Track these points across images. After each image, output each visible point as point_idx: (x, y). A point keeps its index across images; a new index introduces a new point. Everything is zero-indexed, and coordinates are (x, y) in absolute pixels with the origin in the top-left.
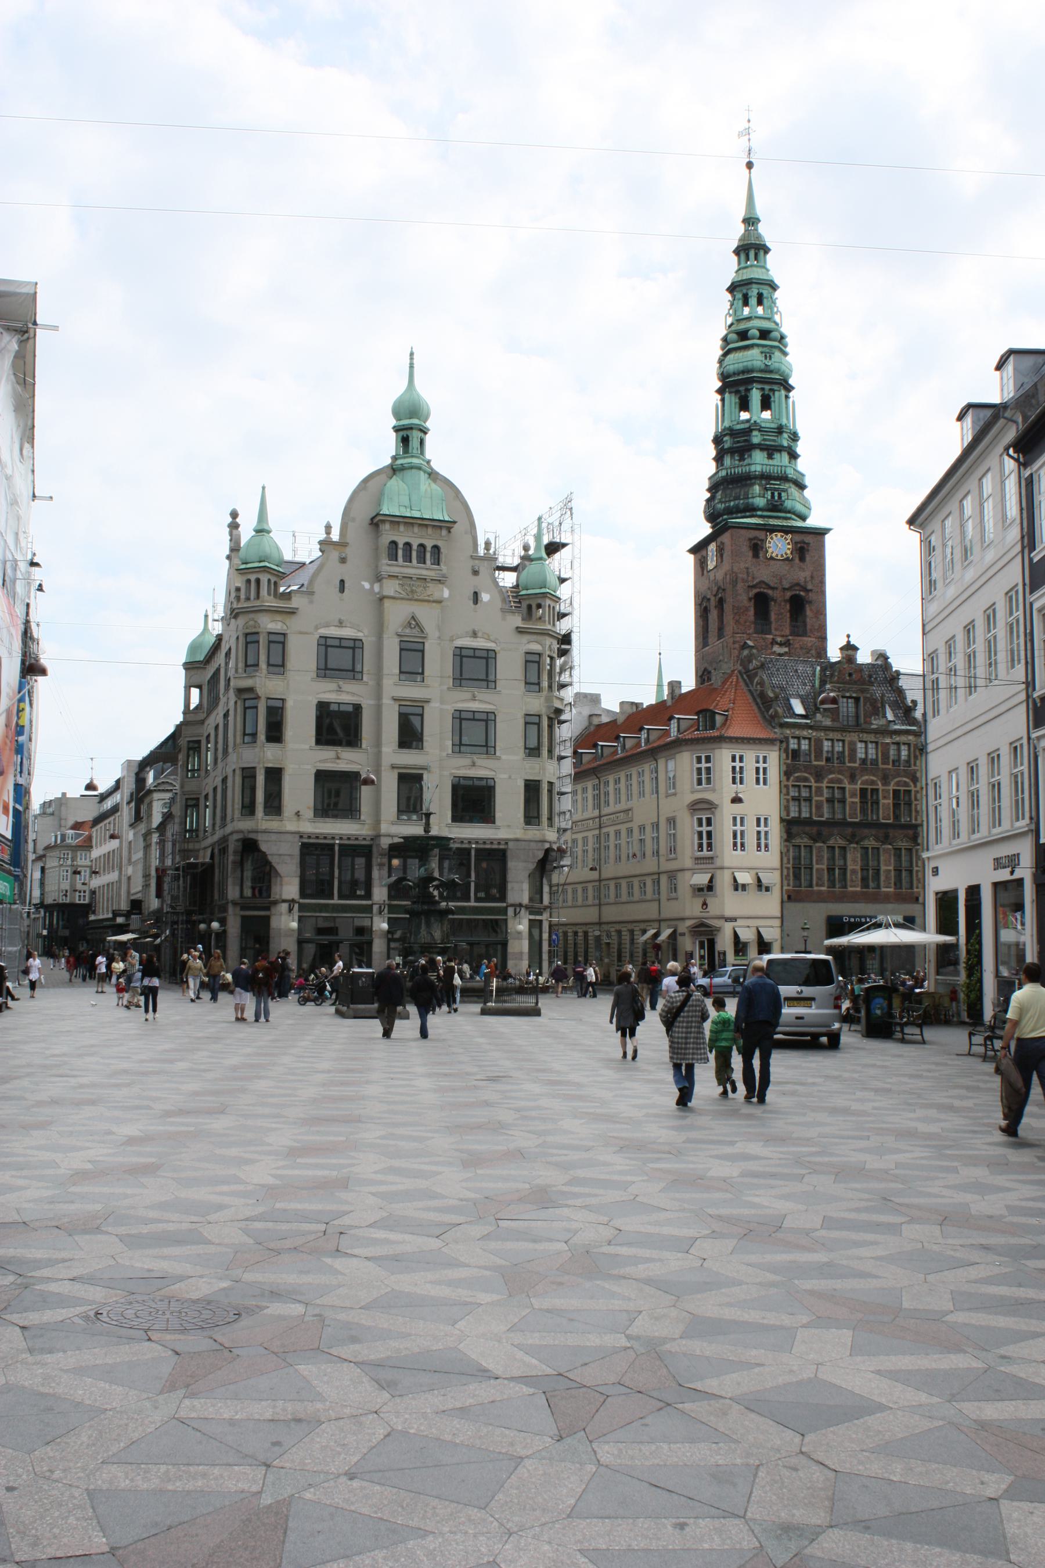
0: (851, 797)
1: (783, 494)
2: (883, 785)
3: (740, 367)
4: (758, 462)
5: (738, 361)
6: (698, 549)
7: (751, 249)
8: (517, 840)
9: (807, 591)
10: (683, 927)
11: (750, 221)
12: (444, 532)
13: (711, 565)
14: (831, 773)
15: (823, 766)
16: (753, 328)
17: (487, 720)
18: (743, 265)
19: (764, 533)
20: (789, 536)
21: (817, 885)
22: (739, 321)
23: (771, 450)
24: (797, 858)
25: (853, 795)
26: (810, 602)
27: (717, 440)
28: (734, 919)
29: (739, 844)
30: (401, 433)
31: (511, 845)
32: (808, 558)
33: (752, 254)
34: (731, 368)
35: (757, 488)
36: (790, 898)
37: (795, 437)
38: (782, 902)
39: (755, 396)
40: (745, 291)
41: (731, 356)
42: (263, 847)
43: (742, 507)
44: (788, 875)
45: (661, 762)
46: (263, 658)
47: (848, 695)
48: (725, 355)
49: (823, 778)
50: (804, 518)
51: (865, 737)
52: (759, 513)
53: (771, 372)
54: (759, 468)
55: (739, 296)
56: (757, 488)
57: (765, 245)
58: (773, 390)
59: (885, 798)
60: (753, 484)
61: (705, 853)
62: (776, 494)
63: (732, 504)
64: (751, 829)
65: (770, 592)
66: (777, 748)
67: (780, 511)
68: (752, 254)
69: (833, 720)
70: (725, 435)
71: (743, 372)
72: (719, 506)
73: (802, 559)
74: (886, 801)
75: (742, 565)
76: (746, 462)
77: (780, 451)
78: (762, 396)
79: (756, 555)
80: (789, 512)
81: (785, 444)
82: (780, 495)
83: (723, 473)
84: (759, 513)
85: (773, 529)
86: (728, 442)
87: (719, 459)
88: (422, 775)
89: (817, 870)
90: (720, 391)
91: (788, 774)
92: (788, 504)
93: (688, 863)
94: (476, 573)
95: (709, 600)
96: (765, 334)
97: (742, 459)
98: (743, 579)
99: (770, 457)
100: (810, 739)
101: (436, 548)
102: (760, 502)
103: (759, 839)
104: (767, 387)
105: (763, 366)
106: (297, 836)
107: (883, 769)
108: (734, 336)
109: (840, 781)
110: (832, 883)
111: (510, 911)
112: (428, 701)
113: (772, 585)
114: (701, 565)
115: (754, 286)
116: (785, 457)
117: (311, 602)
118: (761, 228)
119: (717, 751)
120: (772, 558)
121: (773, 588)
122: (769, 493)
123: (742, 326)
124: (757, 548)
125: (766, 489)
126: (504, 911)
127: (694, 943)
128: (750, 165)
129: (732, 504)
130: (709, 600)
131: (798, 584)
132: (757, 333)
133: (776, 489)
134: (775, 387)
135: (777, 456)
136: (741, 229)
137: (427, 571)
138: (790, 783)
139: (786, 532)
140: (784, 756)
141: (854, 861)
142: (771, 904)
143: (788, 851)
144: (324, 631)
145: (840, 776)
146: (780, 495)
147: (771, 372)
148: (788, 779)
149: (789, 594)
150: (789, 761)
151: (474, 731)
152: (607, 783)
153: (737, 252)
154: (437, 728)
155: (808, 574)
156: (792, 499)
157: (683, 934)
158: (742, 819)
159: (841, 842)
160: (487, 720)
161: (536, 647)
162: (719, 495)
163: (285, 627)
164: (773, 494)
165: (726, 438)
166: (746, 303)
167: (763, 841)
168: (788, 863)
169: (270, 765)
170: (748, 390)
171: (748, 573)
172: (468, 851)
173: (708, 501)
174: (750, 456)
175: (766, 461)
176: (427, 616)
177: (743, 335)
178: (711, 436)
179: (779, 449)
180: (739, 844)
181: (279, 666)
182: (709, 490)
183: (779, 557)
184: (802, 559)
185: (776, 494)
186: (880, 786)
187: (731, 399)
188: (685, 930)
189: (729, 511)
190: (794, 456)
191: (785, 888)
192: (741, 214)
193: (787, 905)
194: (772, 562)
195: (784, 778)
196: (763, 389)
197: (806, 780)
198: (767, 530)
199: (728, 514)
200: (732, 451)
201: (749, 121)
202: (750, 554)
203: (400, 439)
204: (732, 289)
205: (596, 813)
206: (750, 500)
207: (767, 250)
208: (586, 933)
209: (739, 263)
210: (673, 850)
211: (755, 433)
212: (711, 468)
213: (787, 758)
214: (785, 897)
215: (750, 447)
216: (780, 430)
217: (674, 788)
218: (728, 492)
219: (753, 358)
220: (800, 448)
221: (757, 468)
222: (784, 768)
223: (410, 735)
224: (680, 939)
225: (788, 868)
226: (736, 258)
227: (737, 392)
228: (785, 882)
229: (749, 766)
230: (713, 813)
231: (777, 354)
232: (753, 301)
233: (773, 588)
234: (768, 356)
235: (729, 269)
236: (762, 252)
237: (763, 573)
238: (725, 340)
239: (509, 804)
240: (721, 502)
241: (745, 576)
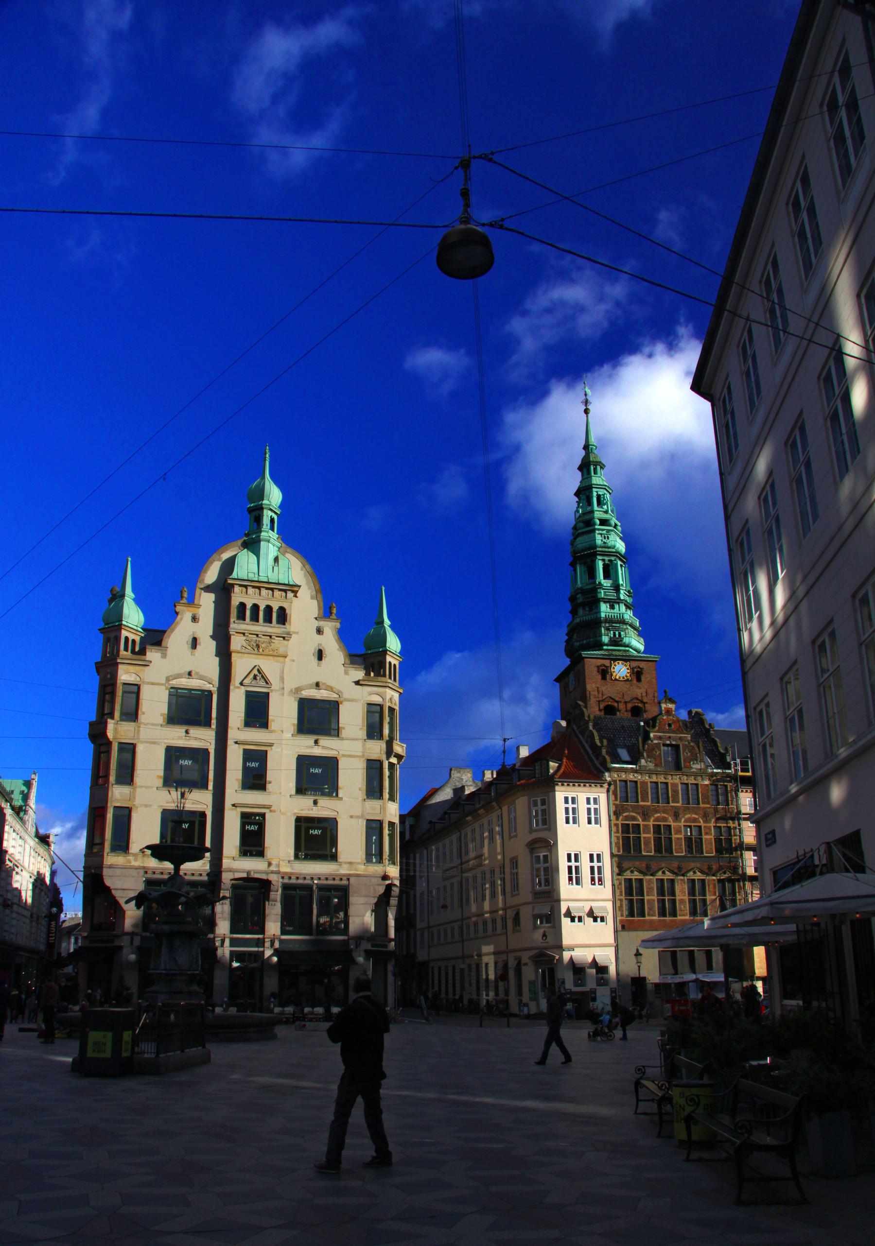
0: (676, 834)
2: (704, 822)
3: (586, 545)
8: (358, 876)
9: (644, 703)
10: (525, 957)
12: (290, 595)
13: (571, 688)
14: (657, 812)
15: (649, 806)
17: (330, 765)
21: (649, 915)
23: (612, 603)
24: (629, 891)
25: (678, 831)
26: (645, 711)
27: (572, 599)
28: (571, 949)
29: (575, 877)
30: (254, 514)
31: (352, 880)
32: (643, 678)
34: (580, 546)
36: (623, 927)
38: (616, 931)
39: (600, 565)
41: (580, 540)
42: (108, 882)
44: (621, 906)
45: (505, 809)
46: (118, 707)
47: (668, 742)
49: (650, 817)
51: (685, 779)
53: (609, 548)
55: (583, 497)
57: (600, 462)
59: (706, 834)
61: (543, 888)
64: (585, 865)
65: (616, 705)
66: (605, 790)
69: (656, 765)
70: (577, 594)
74: (708, 837)
79: (604, 678)
80: (627, 646)
82: (620, 634)
83: (578, 620)
87: (574, 612)
88: (263, 815)
89: (648, 901)
90: (573, 565)
91: (617, 814)
92: (626, 640)
93: (529, 897)
94: (319, 631)
96: (604, 522)
97: (591, 610)
99: (612, 607)
100: (636, 782)
101: (282, 611)
103: (592, 872)
104: (606, 558)
106: (142, 871)
107: (704, 808)
108: (581, 525)
109: (665, 819)
110: (662, 913)
112: (271, 745)
113: (617, 699)
114: (565, 692)
117: (164, 656)
120: (616, 680)
121: (617, 702)
123: (587, 517)
124: (605, 673)
127: (537, 972)
128: (586, 411)
132: (598, 522)
137: (274, 629)
138: (620, 822)
139: (626, 661)
140: (612, 797)
141: (682, 891)
142: (605, 932)
143: (620, 884)
144: (175, 683)
145: (666, 816)
146: (620, 634)
147: (609, 548)
148: (617, 819)
149: (629, 706)
150: (618, 802)
151: (317, 776)
152: (466, 835)
154: (282, 773)
155: (643, 691)
157: (526, 964)
158: (576, 856)
159: (669, 875)
160: (330, 765)
161: (377, 699)
162: (575, 637)
163: (138, 679)
164: (614, 634)
165: (579, 596)
166: (589, 502)
167: (596, 876)
168: (621, 895)
169: (118, 805)
172: (309, 888)
173: (567, 641)
176: (269, 667)
179: (618, 601)
180: (575, 877)
181: (132, 715)
184: (639, 680)
186: (702, 824)
188: (527, 961)
191: (618, 918)
192: (583, 443)
193: (624, 934)
195: (613, 817)
196: (603, 560)
197: (634, 819)
198: (611, 659)
200: (583, 605)
202: (600, 677)
203: (253, 518)
204: (577, 494)
205: (459, 862)
208: (454, 968)
209: (582, 476)
210: (516, 886)
213: (616, 799)
214: (619, 928)
216: (617, 588)
217: (516, 831)
222: (613, 808)
223: (256, 777)
224: (524, 968)
225: (621, 900)
226: (580, 473)
227: (585, 563)
228: (619, 913)
229: (582, 807)
230: (550, 851)
235: (575, 481)
237: (609, 690)
239: (351, 843)
240: (577, 641)
241: (596, 693)
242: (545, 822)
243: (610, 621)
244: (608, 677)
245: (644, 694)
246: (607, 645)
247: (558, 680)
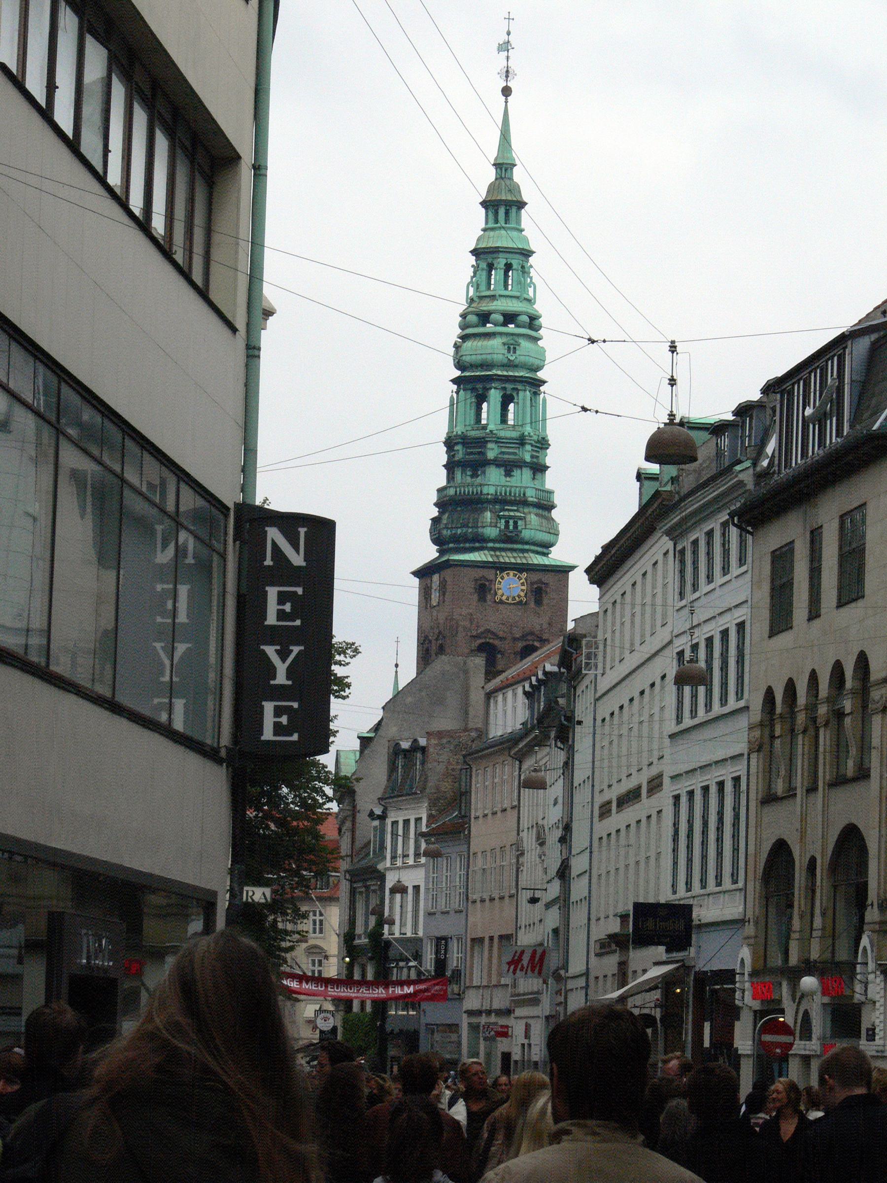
1: (520, 523)
4: (493, 481)
5: (476, 349)
6: (423, 573)
7: (503, 204)
11: (504, 168)
16: (495, 312)
18: (491, 225)
19: (493, 571)
20: (524, 575)
22: (481, 298)
23: (509, 467)
27: (450, 443)
32: (545, 601)
33: (502, 211)
35: (488, 515)
37: (543, 444)
40: (490, 261)
41: (469, 344)
48: (464, 338)
50: (545, 547)
52: (490, 545)
54: (492, 490)
55: (484, 265)
56: (488, 515)
58: (517, 390)
60: (485, 509)
62: (511, 522)
63: (459, 531)
65: (497, 642)
67: (516, 542)
68: (502, 211)
72: (445, 532)
73: (539, 602)
75: (465, 611)
76: (479, 480)
77: (521, 467)
78: (503, 397)
79: (482, 598)
81: (528, 458)
82: (515, 523)
83: (451, 492)
84: (490, 545)
85: (503, 568)
87: (450, 467)
92: (526, 534)
95: (430, 642)
96: (510, 318)
97: (474, 475)
98: (465, 628)
99: (508, 474)
102: (491, 532)
104: (509, 386)
105: (505, 361)
113: (501, 634)
115: (501, 255)
116: (527, 473)
118: (518, 175)
119: (328, 908)
121: (501, 639)
122: (503, 521)
123: (485, 306)
124: (483, 589)
125: (500, 517)
128: (506, 92)
129: (459, 531)
130: (430, 642)
131: (532, 633)
133: (511, 517)
135: (517, 473)
136: (491, 175)
146: (515, 523)
153: (485, 204)
155: (544, 620)
156: (531, 526)
164: (507, 523)
170: (487, 390)
171: (471, 621)
173: (435, 521)
174: (484, 473)
175: (503, 480)
177: (484, 318)
178: (443, 437)
179: (520, 464)
182: (436, 505)
183: (510, 601)
184: (539, 602)
185: (511, 522)
187: (468, 397)
189: (455, 539)
190: (539, 469)
192: (493, 154)
194: (501, 607)
196: (504, 389)
198: (497, 568)
199: (454, 542)
200: (463, 465)
201: (509, 33)
202: (475, 597)
204: (476, 252)
206: (480, 530)
207: (521, 205)
211: (490, 445)
212: (441, 479)
215: (487, 463)
216: (522, 441)
218: (456, 516)
219: (494, 349)
220: (551, 458)
221: (490, 490)
227: (473, 390)
231: (524, 344)
233: (501, 639)
234: (512, 348)
236: (514, 209)
238: (464, 316)
241: (467, 624)
242: (321, 931)
243: (501, 501)
244: (489, 597)
245: (545, 626)
246: (493, 541)
247: (418, 573)
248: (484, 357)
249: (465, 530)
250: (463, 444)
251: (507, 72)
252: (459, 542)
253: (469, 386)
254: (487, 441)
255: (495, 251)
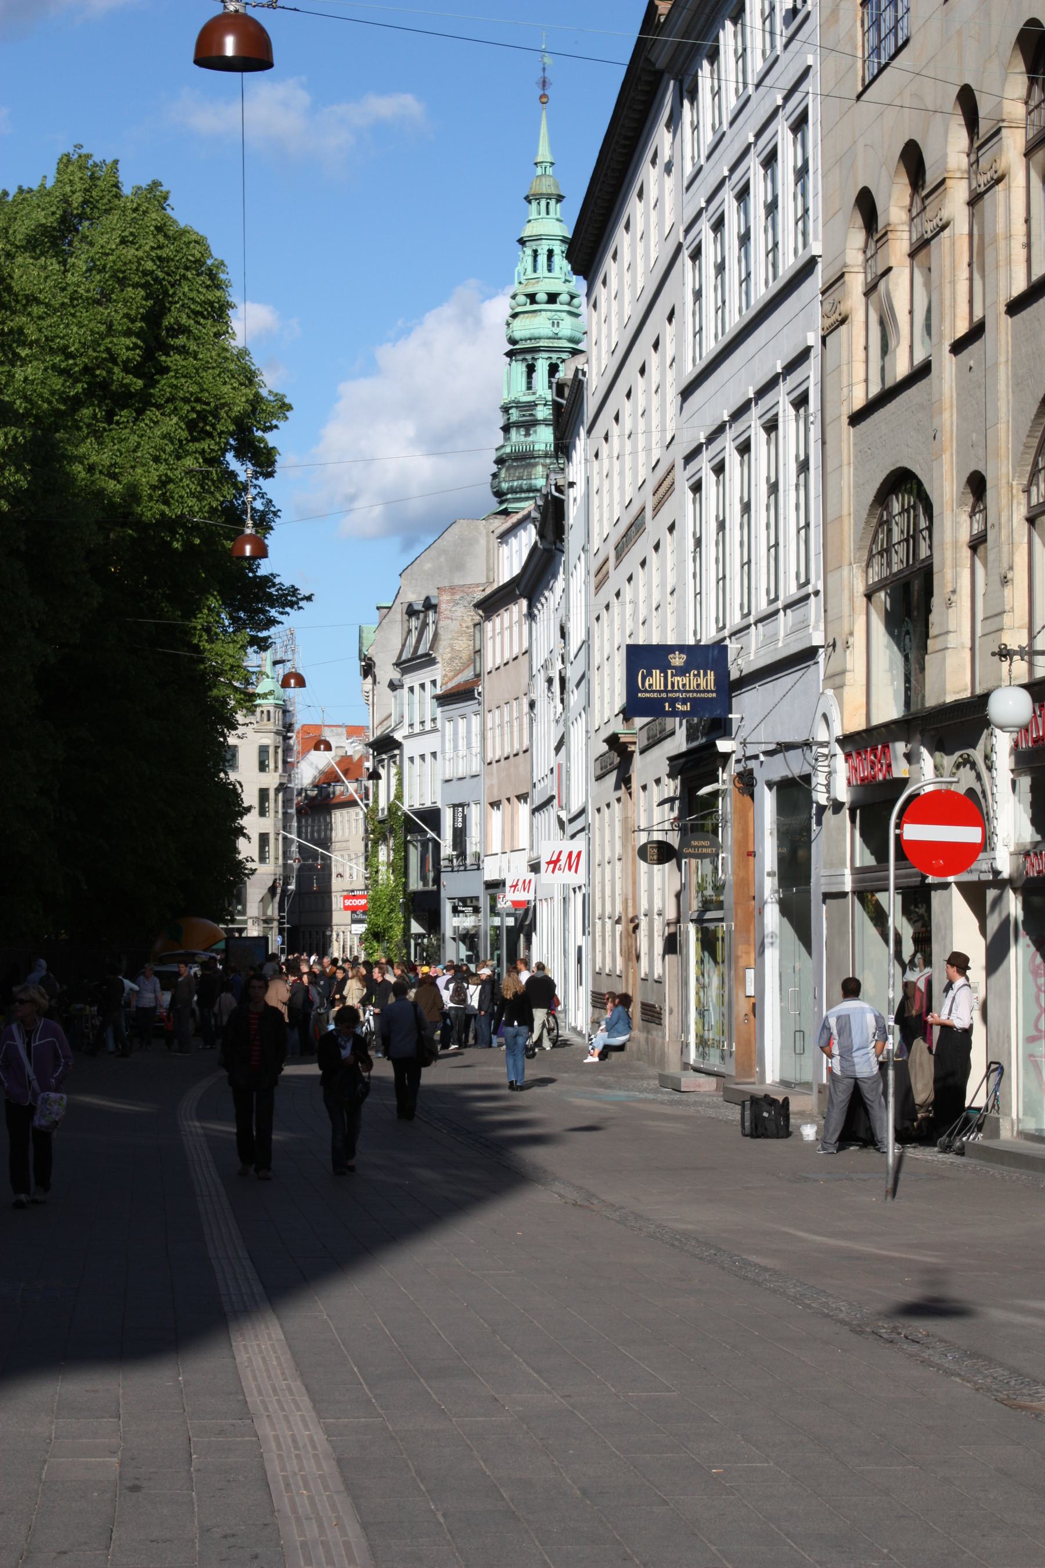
3: (526, 334)
34: (517, 335)
40: (534, 248)
43: (525, 487)
60: (535, 465)
63: (515, 483)
71: (530, 339)
76: (530, 439)
83: (508, 450)
86: (515, 415)
87: (506, 429)
96: (552, 298)
97: (527, 434)
104: (554, 356)
105: (550, 334)
111: (250, 922)
126: (245, 922)
129: (515, 483)
134: (564, 356)
174: (535, 432)
177: (532, 298)
189: (512, 490)
199: (512, 493)
200: (518, 425)
206: (533, 482)
211: (540, 408)
218: (512, 471)
232: (542, 259)
248: (532, 331)
249: (520, 482)
250: (517, 407)
251: (544, 82)
252: (516, 493)
253: (520, 357)
254: (536, 405)
255: (539, 238)
